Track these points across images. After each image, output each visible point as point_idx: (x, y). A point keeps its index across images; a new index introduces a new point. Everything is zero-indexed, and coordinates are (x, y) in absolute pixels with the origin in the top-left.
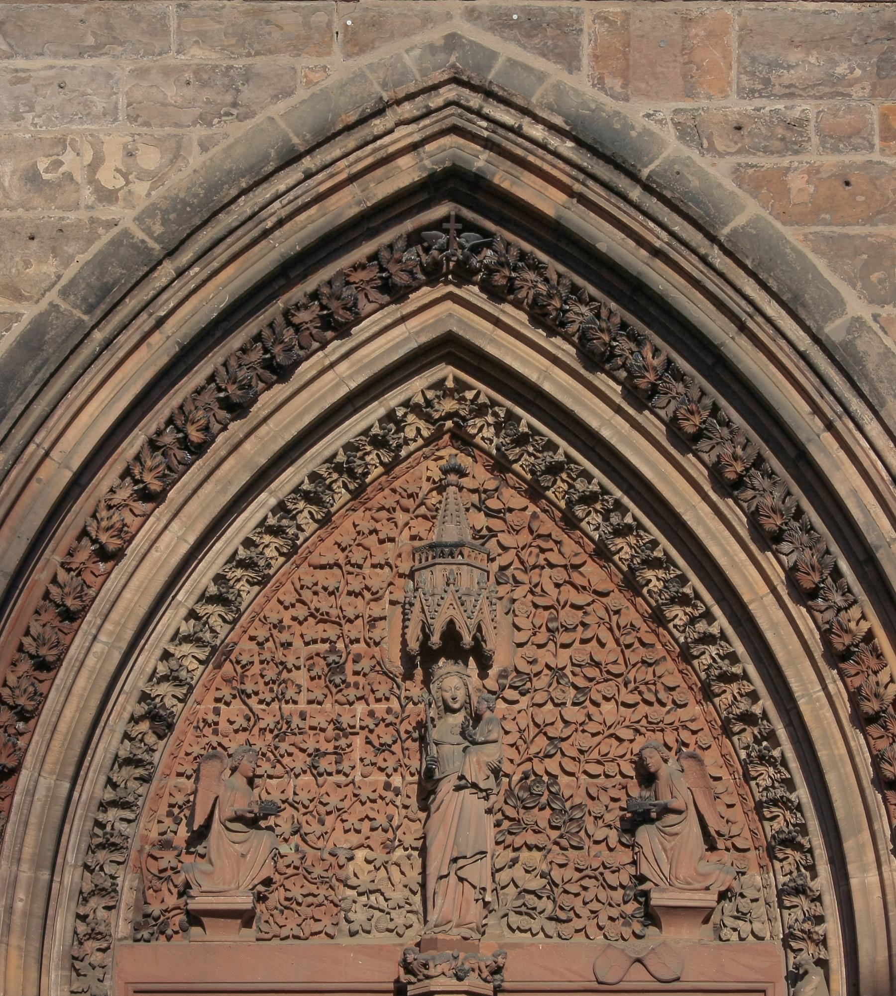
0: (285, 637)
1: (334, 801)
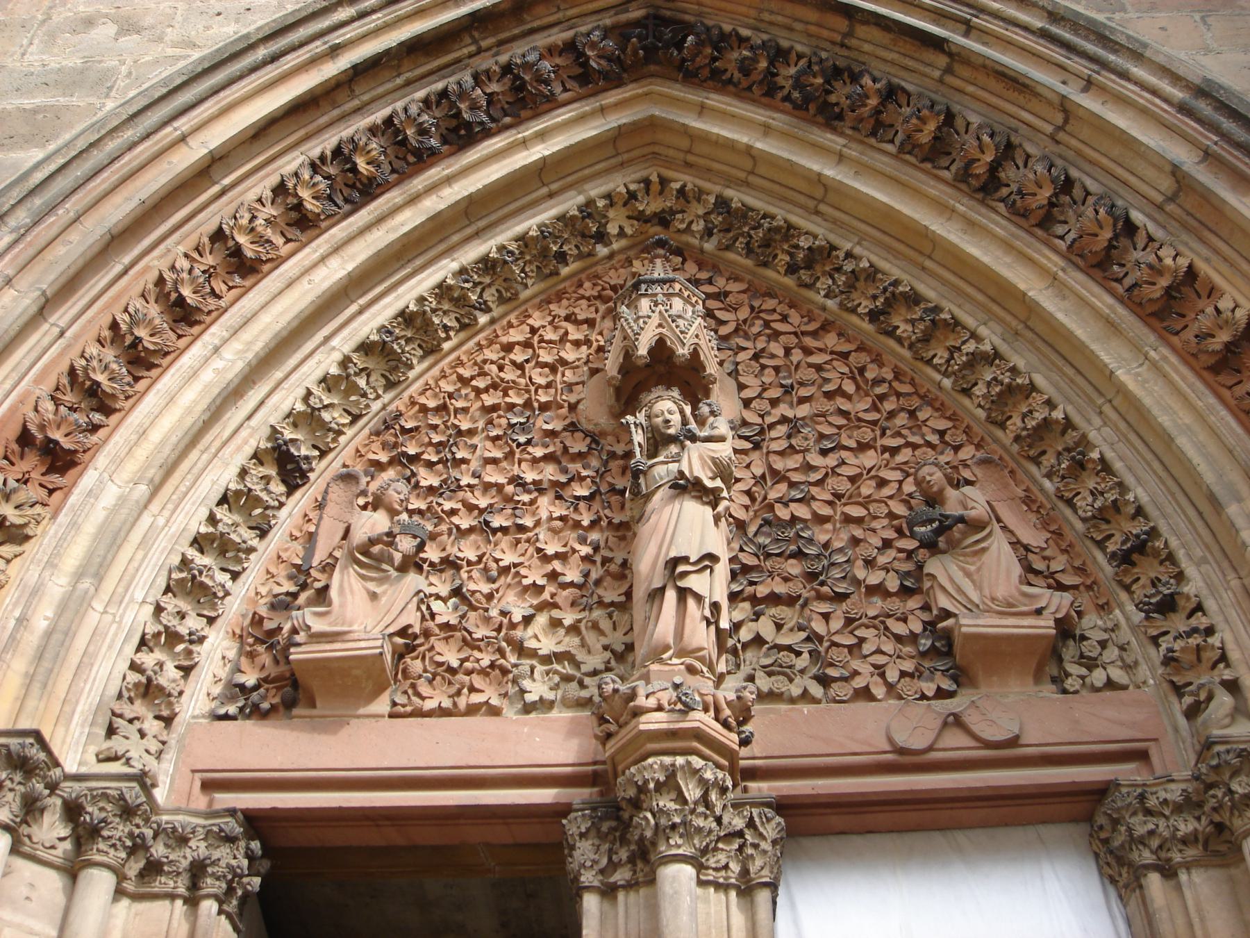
0: (460, 404)
1: (508, 558)
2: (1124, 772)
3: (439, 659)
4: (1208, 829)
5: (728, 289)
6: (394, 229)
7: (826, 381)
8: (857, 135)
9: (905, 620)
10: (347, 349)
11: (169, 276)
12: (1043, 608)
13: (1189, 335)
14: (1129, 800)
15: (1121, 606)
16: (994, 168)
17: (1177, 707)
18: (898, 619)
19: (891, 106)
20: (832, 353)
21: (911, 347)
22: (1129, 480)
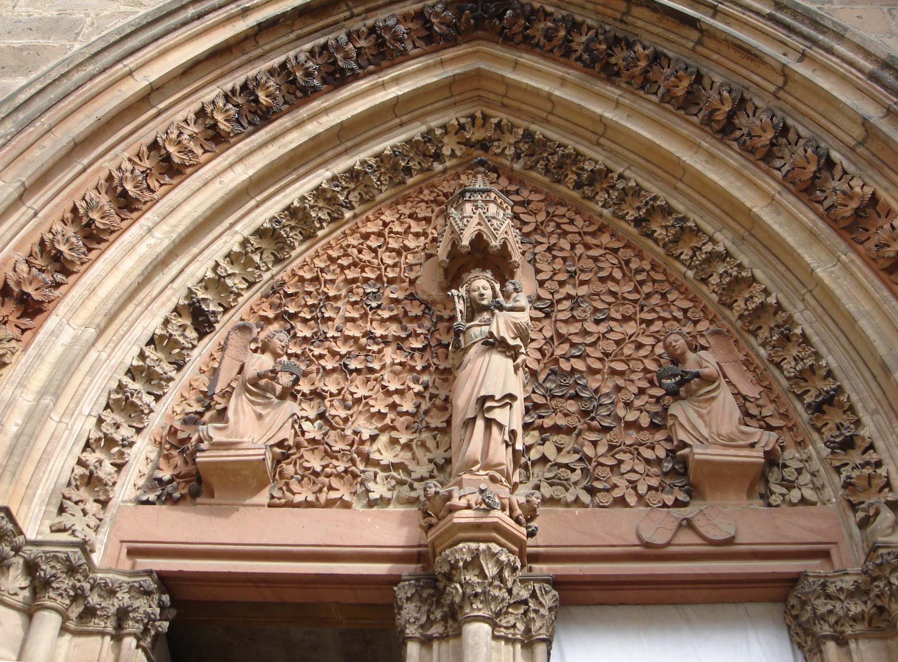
0: (329, 277)
1: (361, 392)
2: (812, 566)
3: (306, 464)
4: (872, 611)
5: (530, 198)
6: (285, 146)
7: (601, 269)
8: (630, 88)
9: (653, 448)
10: (246, 233)
11: (116, 174)
12: (755, 443)
13: (871, 244)
14: (815, 587)
15: (813, 443)
16: (731, 115)
17: (853, 520)
18: (648, 447)
19: (656, 68)
20: (606, 248)
21: (664, 246)
22: (823, 350)
